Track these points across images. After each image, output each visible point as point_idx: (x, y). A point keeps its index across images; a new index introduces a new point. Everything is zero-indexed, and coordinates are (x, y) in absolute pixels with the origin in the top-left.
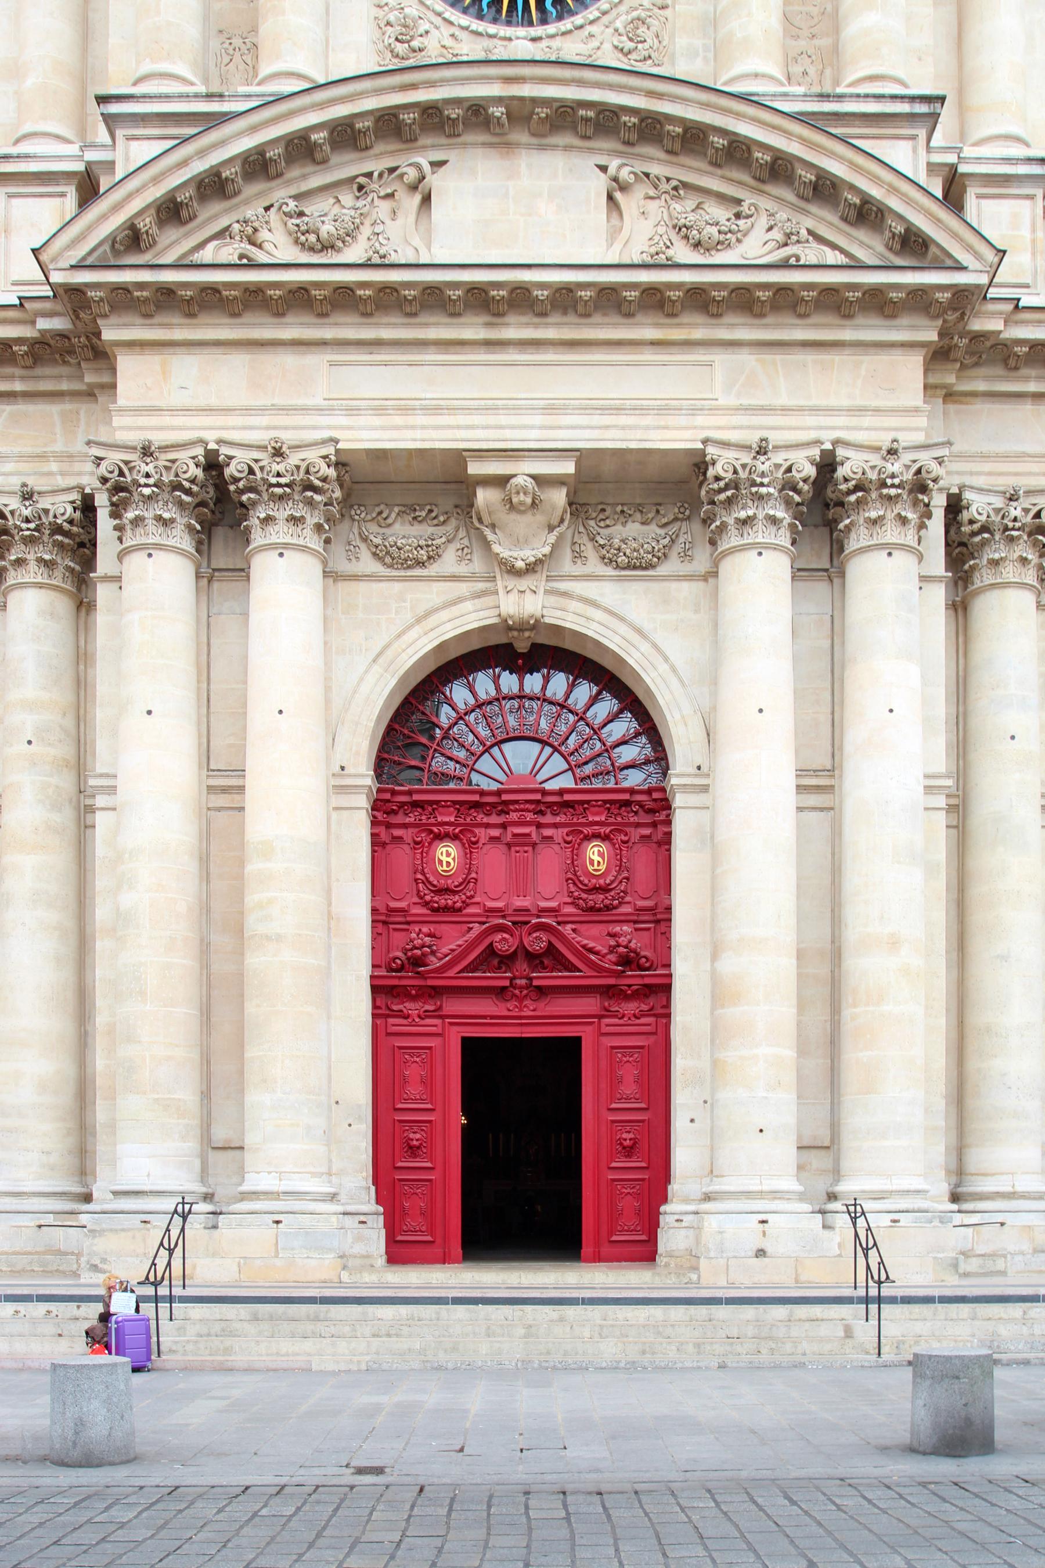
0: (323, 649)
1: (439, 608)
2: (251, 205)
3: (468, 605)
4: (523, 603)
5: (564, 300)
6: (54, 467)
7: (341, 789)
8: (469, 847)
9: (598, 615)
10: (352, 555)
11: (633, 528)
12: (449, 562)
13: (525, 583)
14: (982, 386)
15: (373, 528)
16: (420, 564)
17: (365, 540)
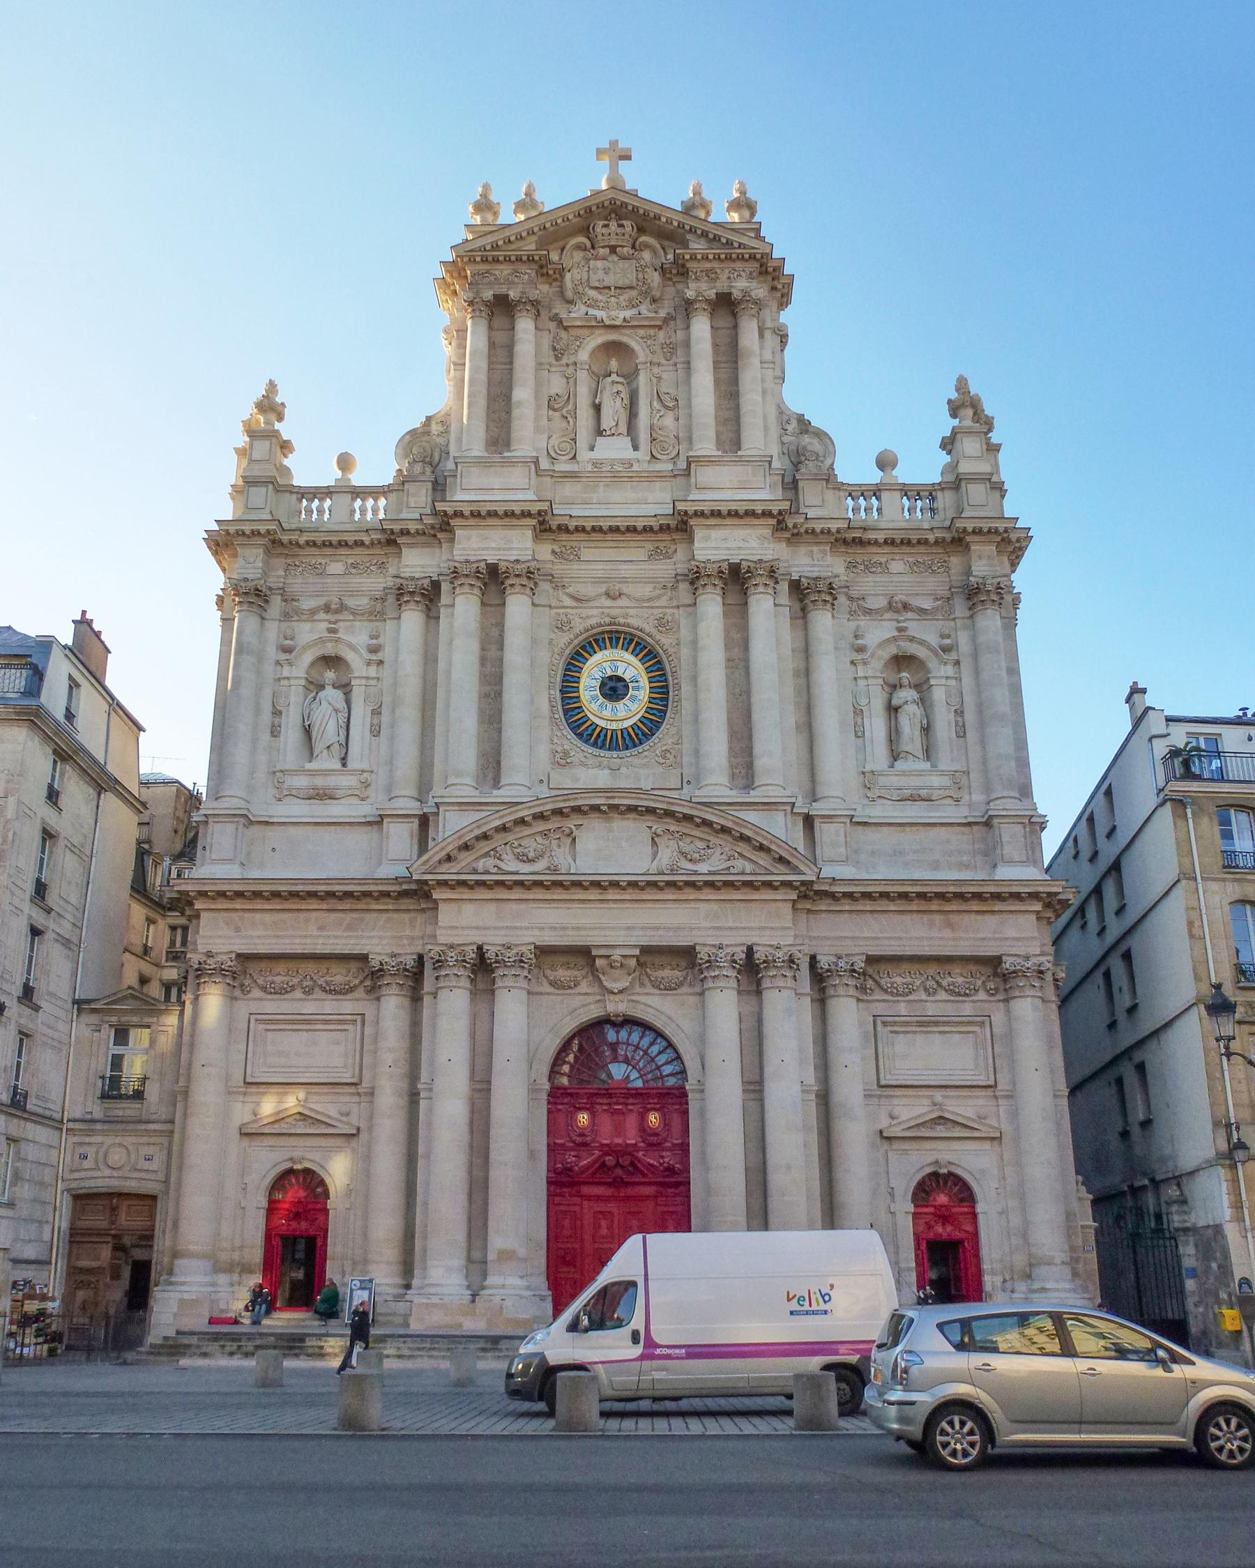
0: (529, 1026)
1: (578, 1006)
2: (500, 838)
3: (592, 1006)
4: (618, 1006)
5: (633, 885)
6: (405, 942)
7: (535, 1090)
8: (593, 1115)
9: (651, 1011)
10: (539, 984)
11: (666, 973)
12: (584, 987)
13: (617, 998)
14: (824, 908)
15: (548, 972)
16: (570, 987)
17: (546, 977)
